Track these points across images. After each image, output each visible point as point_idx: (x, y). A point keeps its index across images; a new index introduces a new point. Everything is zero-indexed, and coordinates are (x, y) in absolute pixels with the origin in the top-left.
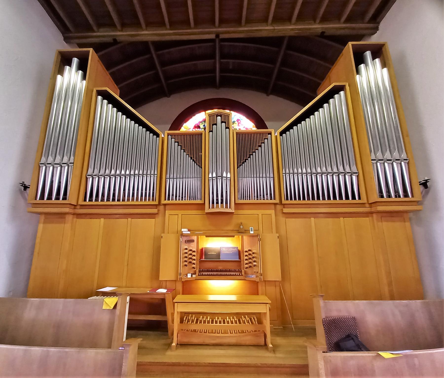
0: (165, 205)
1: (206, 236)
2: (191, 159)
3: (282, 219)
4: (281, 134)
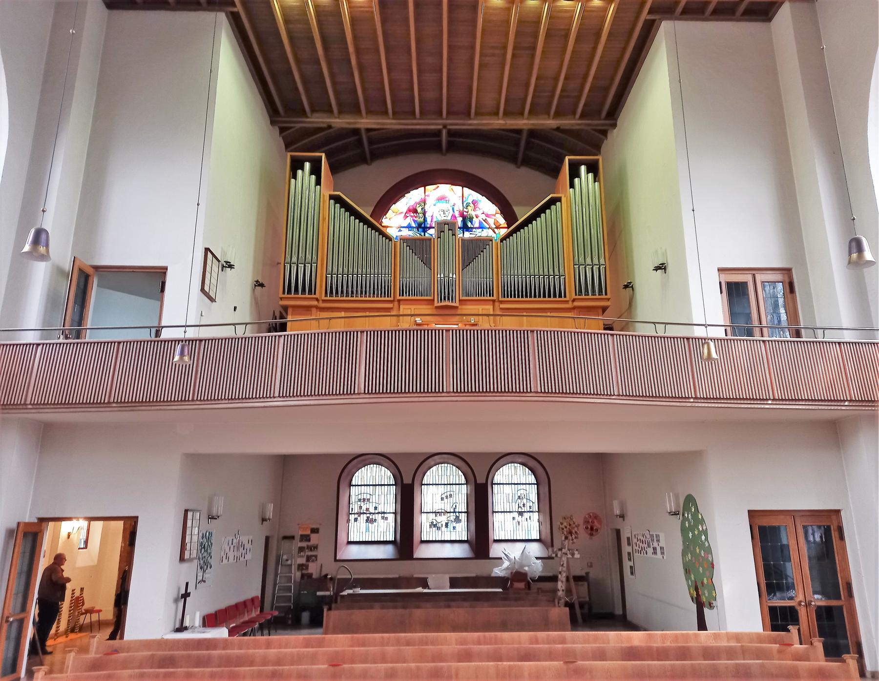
0: (399, 301)
4: (502, 241)
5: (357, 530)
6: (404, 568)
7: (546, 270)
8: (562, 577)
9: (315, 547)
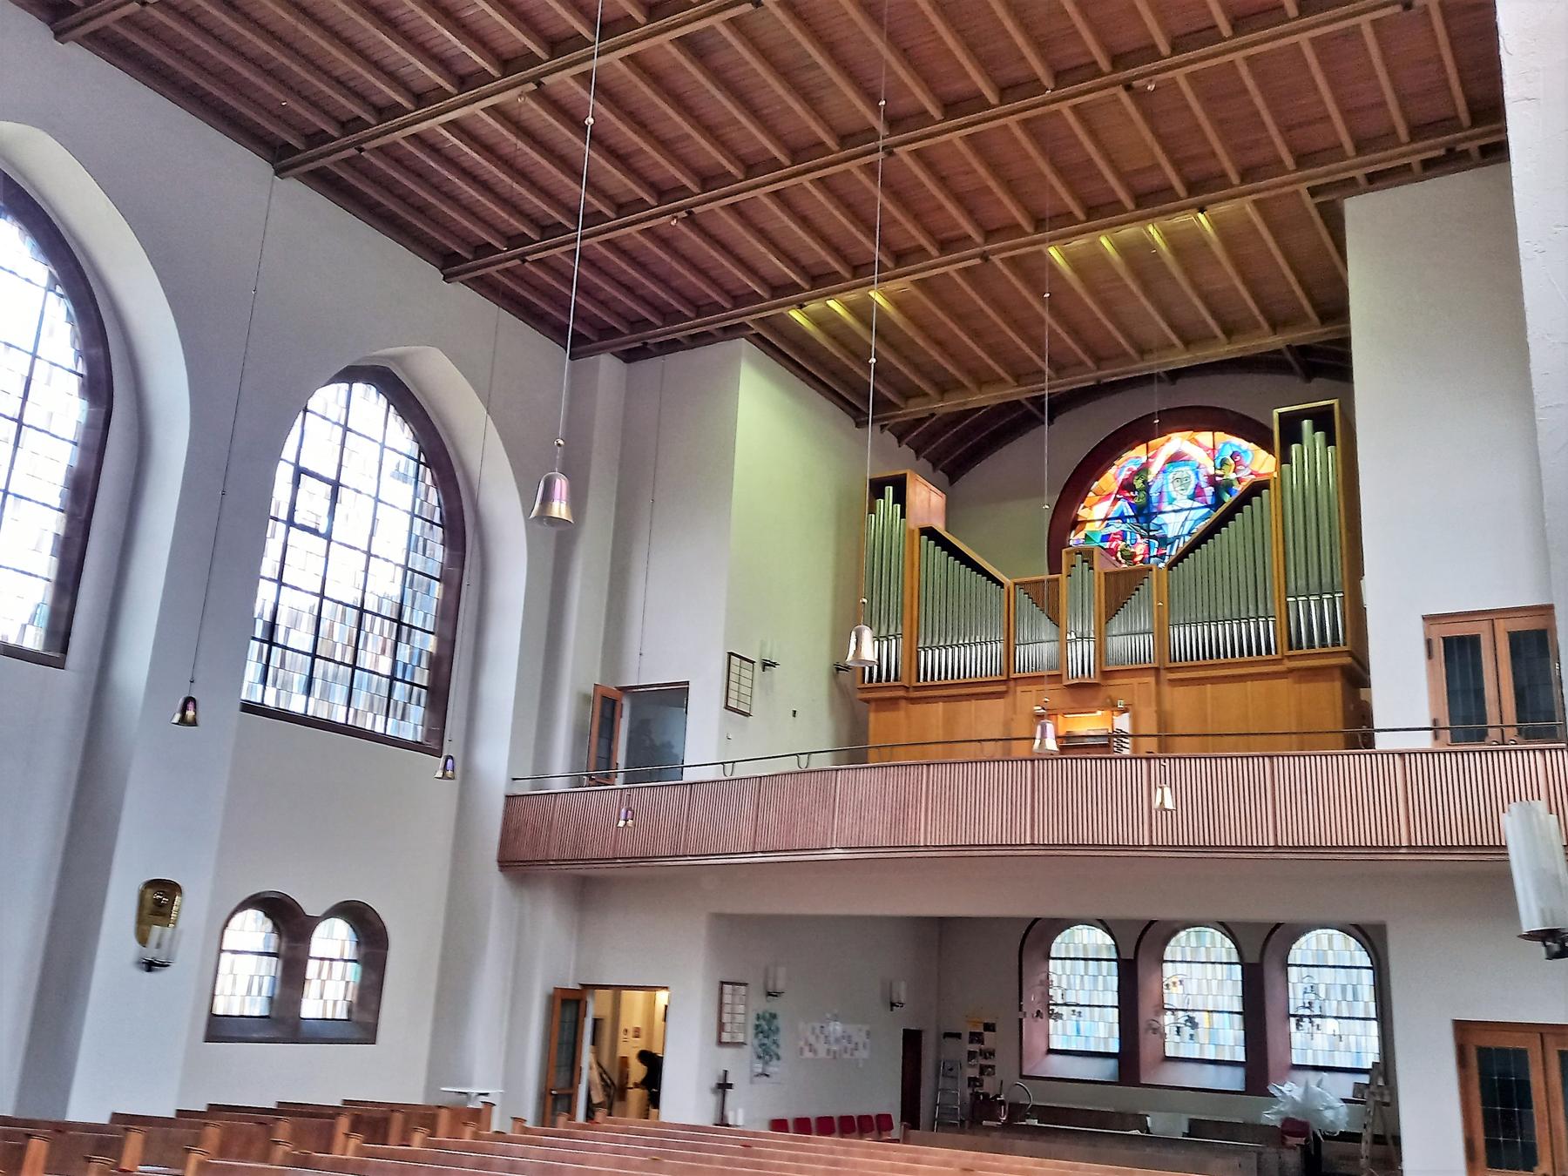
3: (1166, 689)
4: (1170, 567)
5: (1061, 1034)
6: (1125, 1099)
7: (1243, 608)
8: (1367, 1136)
9: (992, 1053)
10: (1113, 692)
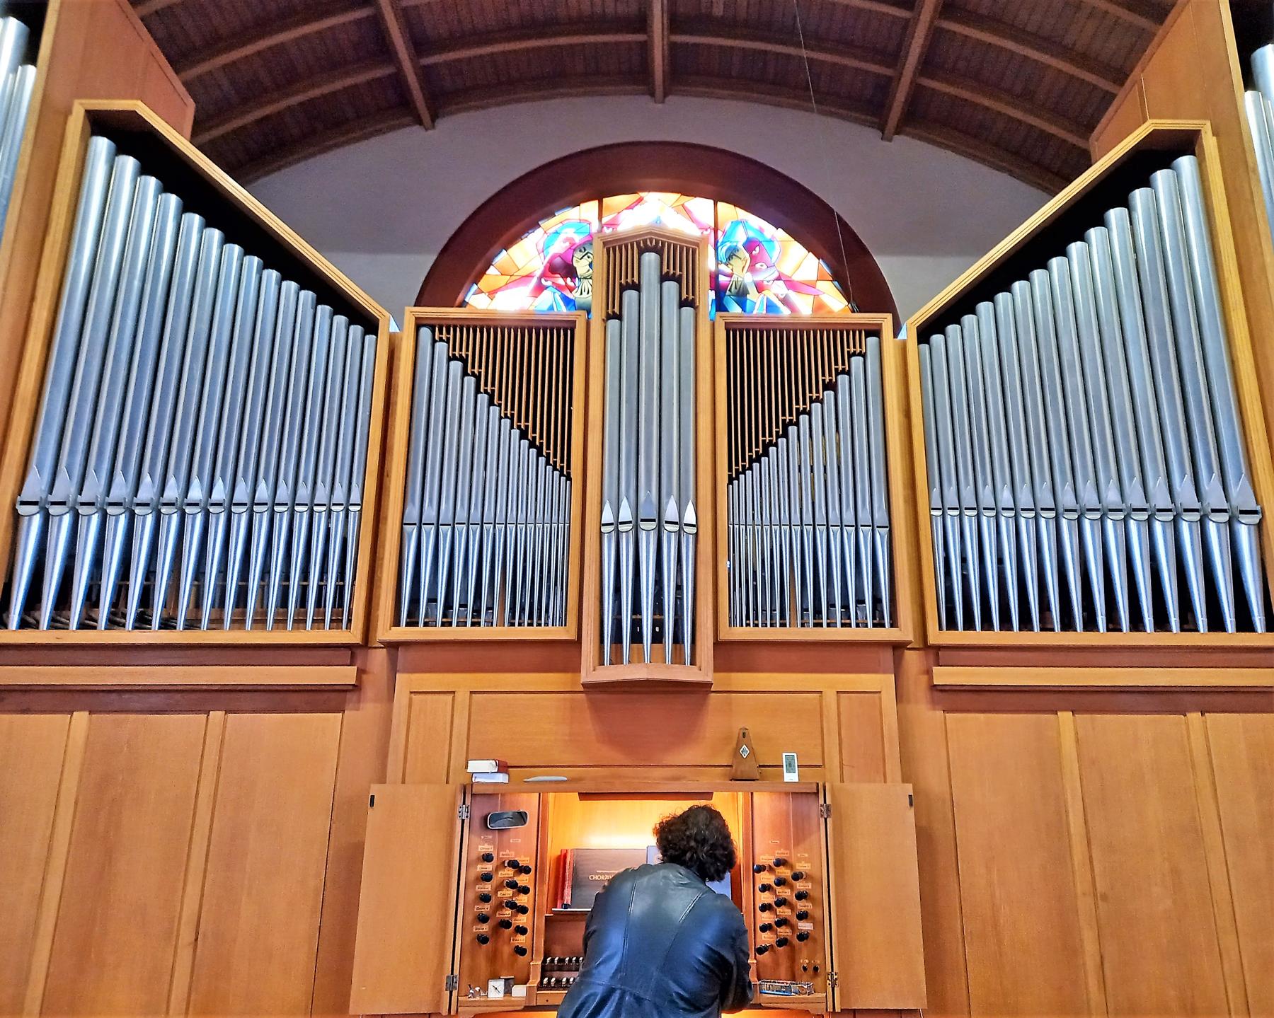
0: (393, 646)
1: (584, 796)
2: (524, 435)
3: (928, 717)
4: (924, 334)
10: (745, 715)
